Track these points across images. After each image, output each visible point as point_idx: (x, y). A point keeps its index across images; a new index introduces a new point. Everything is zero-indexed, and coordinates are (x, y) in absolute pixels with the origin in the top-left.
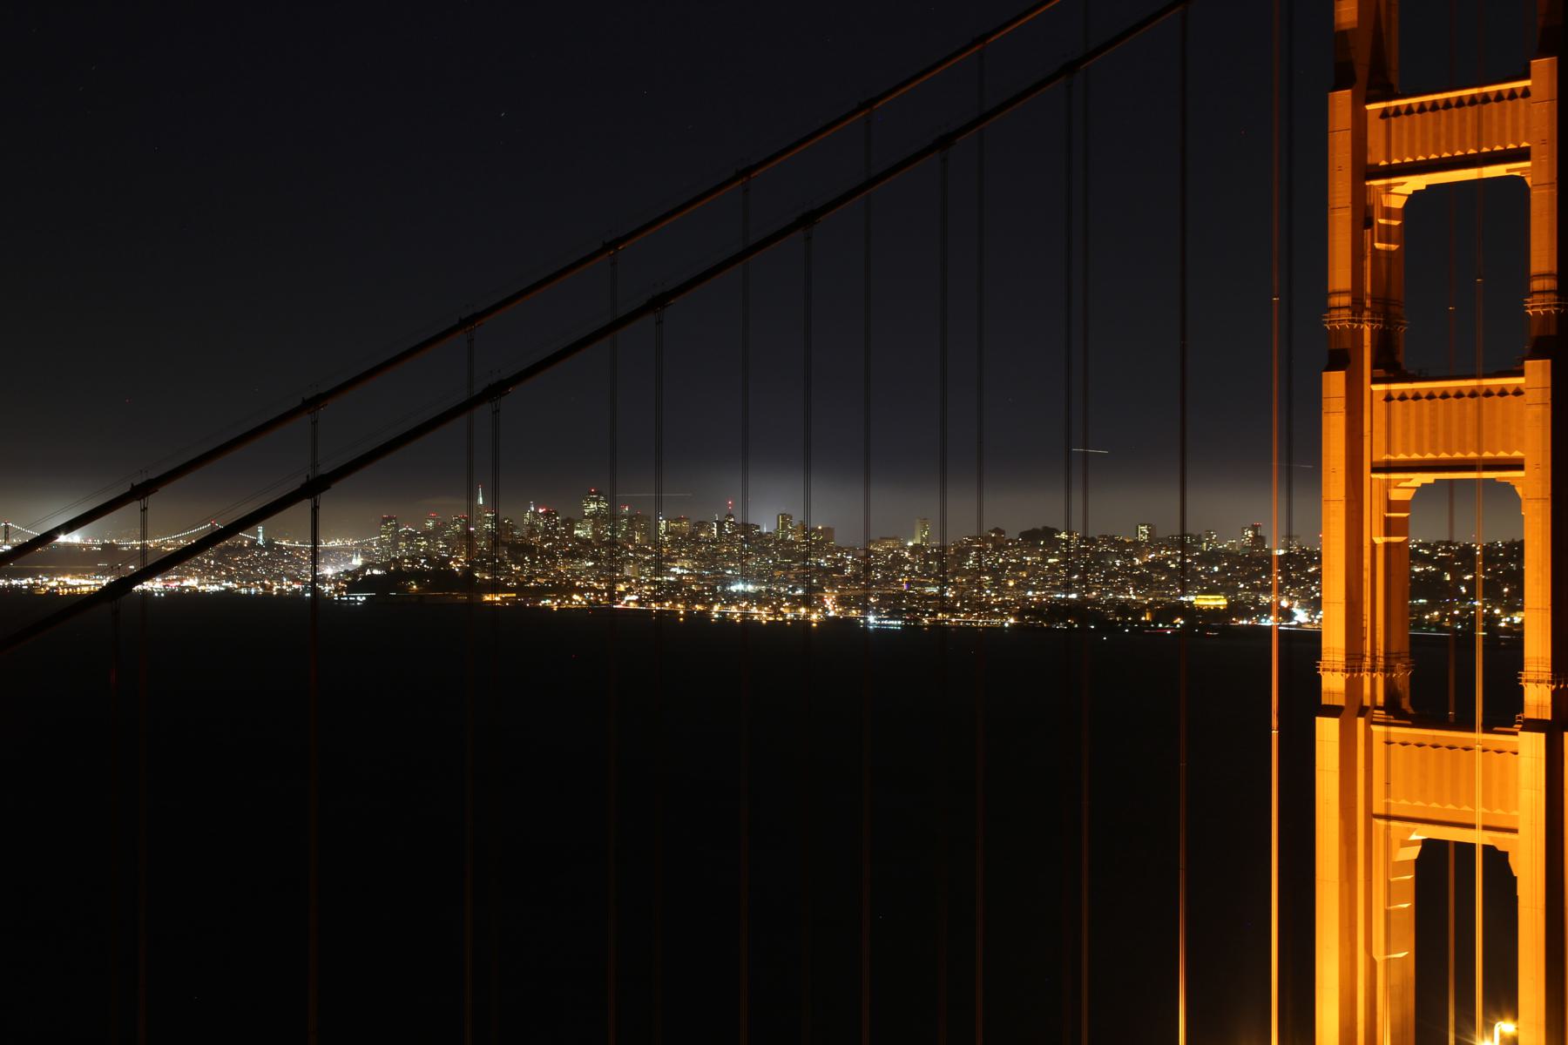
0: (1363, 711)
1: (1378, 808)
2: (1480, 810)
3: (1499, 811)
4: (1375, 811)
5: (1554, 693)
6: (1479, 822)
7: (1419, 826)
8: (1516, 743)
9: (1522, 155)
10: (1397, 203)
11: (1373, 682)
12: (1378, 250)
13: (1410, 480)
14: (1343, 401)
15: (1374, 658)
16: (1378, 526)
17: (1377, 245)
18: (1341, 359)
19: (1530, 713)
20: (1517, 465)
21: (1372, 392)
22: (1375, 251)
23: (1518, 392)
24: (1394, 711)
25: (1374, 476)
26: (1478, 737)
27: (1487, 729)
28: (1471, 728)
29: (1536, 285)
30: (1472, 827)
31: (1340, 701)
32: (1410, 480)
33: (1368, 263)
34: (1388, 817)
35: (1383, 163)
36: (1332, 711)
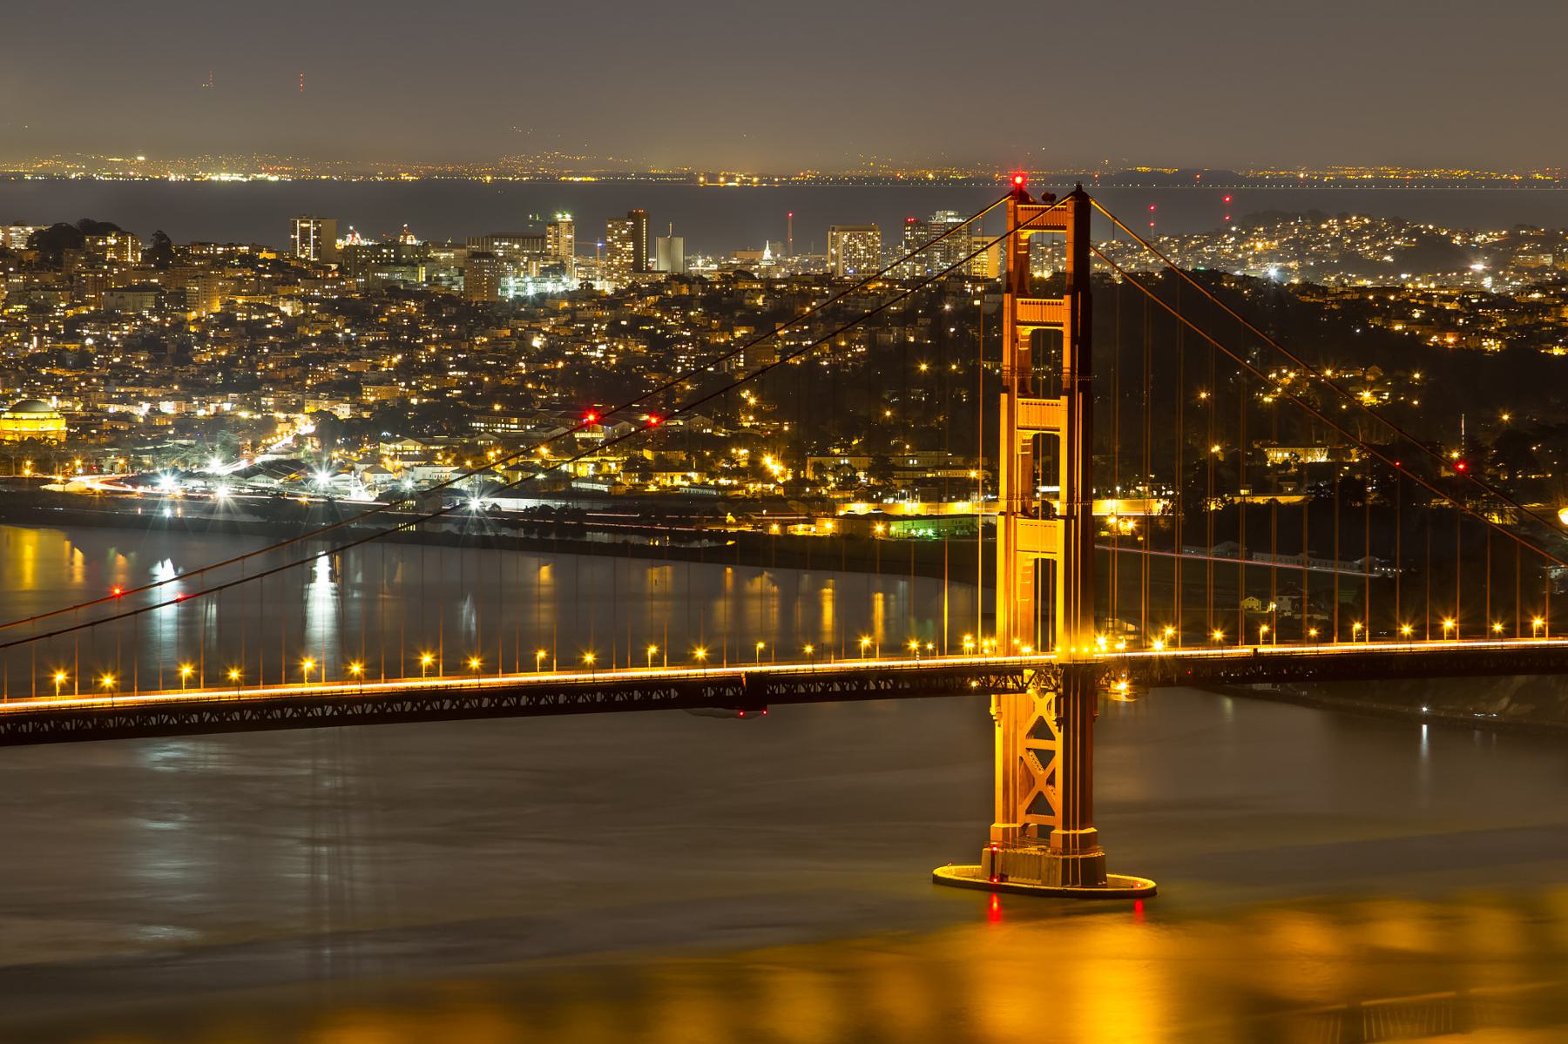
0: (1013, 514)
5: (1068, 507)
9: (1061, 325)
10: (1029, 333)
11: (1017, 503)
15: (1017, 495)
16: (1019, 449)
18: (1007, 390)
19: (1058, 513)
20: (1058, 430)
22: (1019, 350)
24: (1025, 512)
26: (1040, 521)
27: (1043, 519)
29: (1065, 371)
31: (1005, 511)
36: (1001, 514)
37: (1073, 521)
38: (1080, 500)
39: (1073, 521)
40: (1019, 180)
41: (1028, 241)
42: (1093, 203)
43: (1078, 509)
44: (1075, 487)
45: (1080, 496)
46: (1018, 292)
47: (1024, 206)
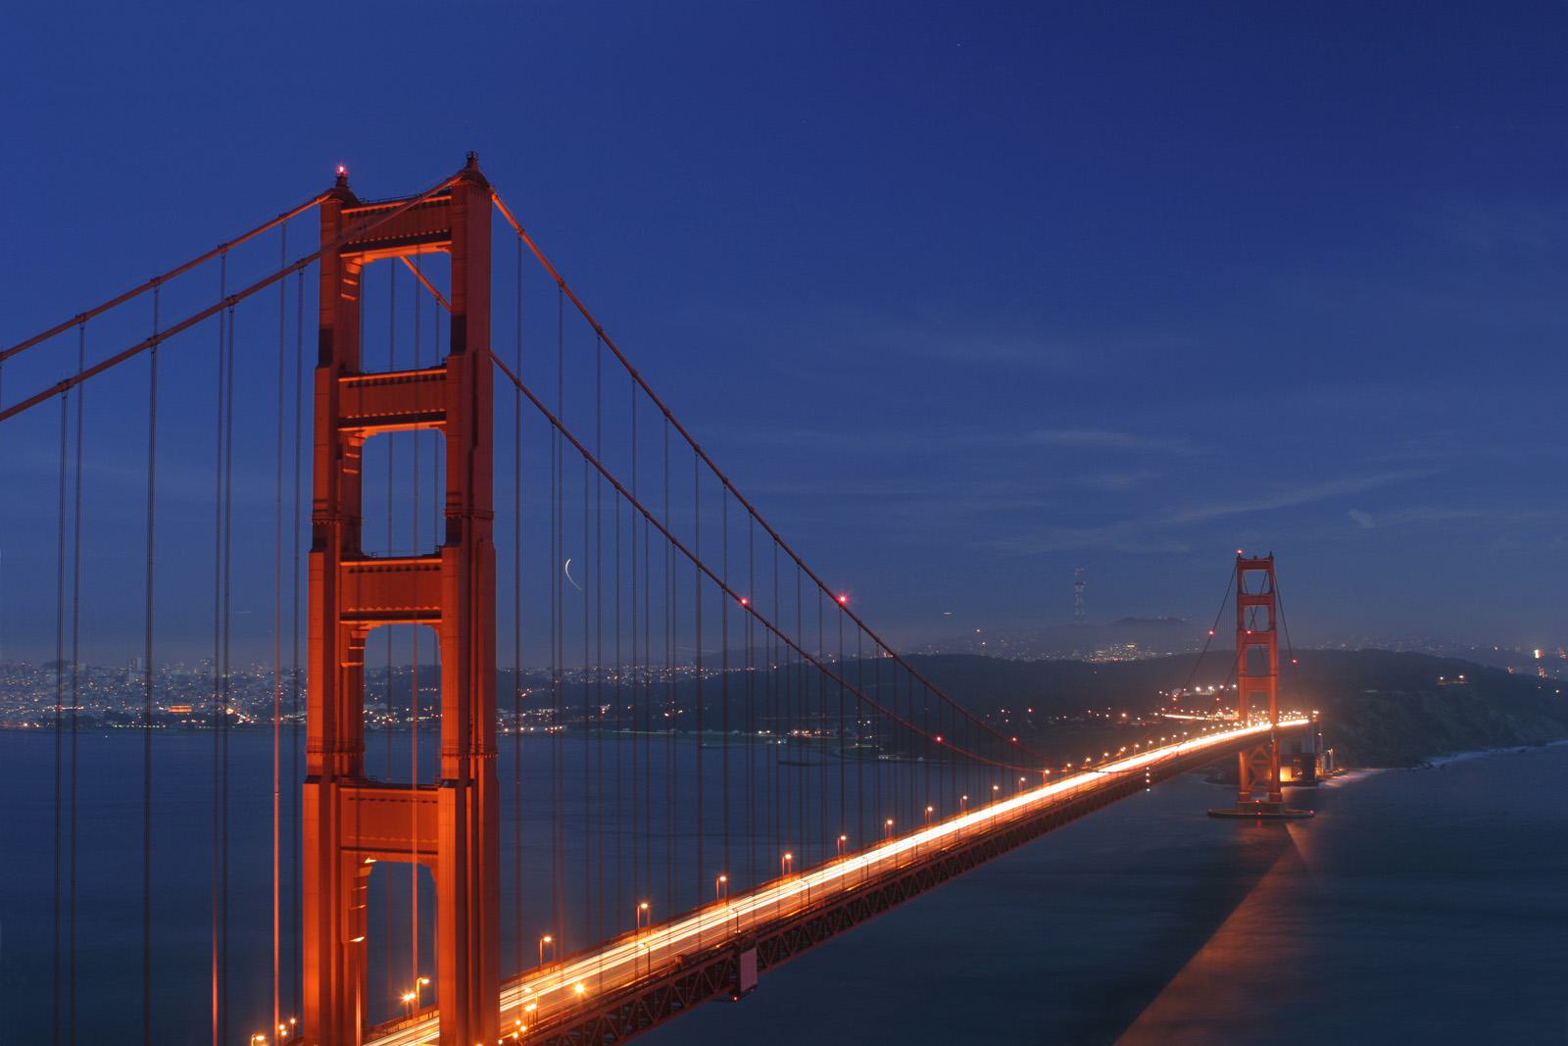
0: (334, 778)
1: (348, 839)
2: (415, 841)
3: (424, 841)
4: (343, 844)
6: (415, 848)
7: (372, 853)
8: (436, 796)
12: (346, 474)
13: (365, 625)
14: (322, 573)
15: (341, 742)
17: (345, 470)
23: (437, 568)
24: (355, 776)
25: (342, 622)
26: (414, 792)
27: (419, 788)
28: (410, 787)
30: (411, 852)
31: (320, 773)
32: (365, 625)
33: (339, 482)
34: (358, 849)
35: (350, 417)
37: (469, 789)
38: (482, 751)
39: (469, 789)
40: (342, 169)
41: (356, 277)
42: (493, 197)
43: (479, 766)
44: (473, 722)
45: (481, 742)
46: (342, 366)
47: (355, 210)
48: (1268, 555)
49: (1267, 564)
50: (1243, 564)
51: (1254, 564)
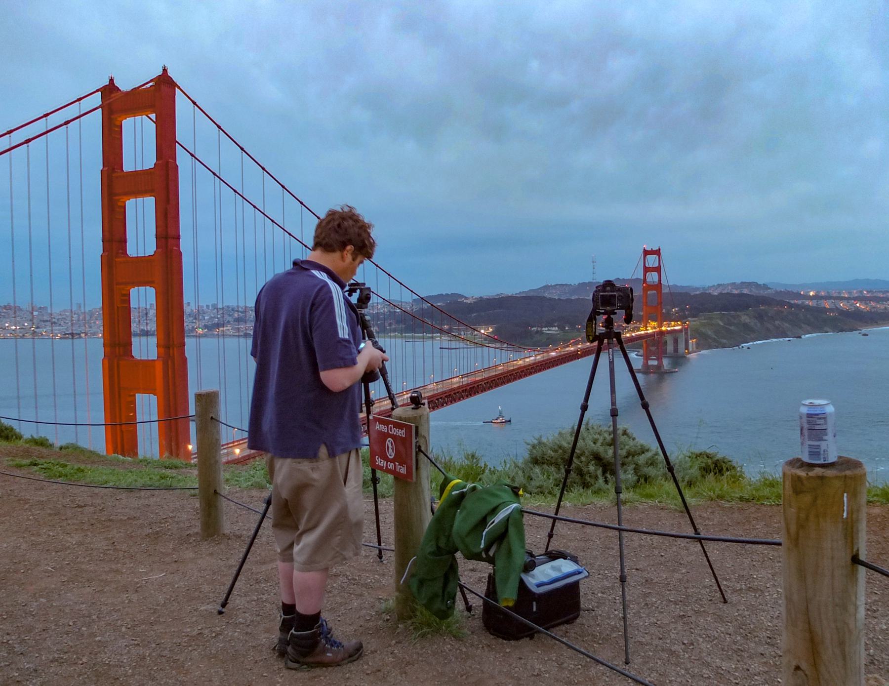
21: (116, 261)
25: (118, 286)
48: (658, 248)
49: (657, 252)
50: (646, 253)
51: (652, 252)
